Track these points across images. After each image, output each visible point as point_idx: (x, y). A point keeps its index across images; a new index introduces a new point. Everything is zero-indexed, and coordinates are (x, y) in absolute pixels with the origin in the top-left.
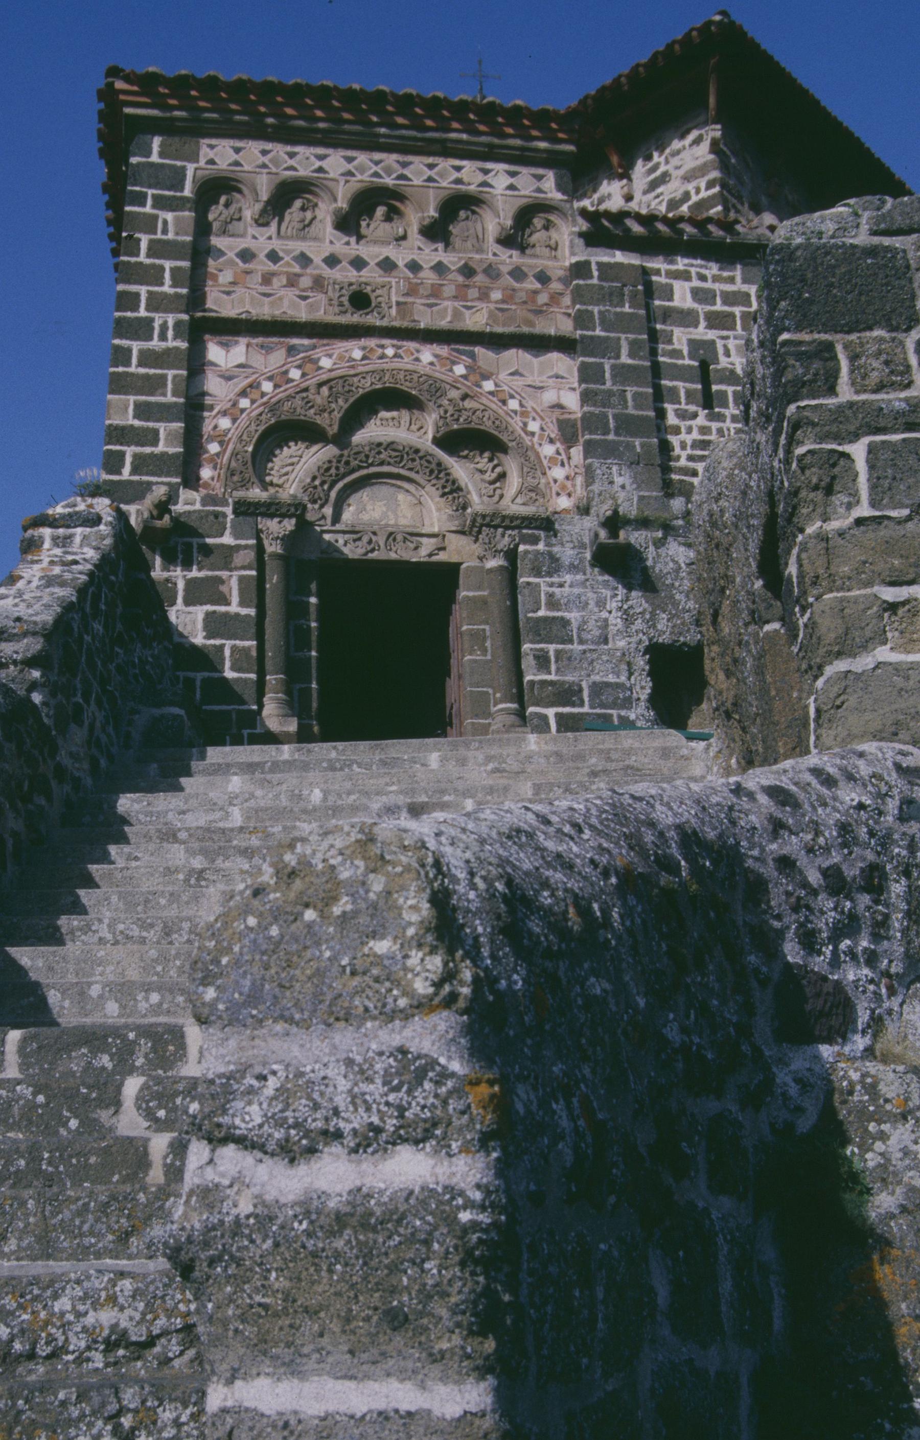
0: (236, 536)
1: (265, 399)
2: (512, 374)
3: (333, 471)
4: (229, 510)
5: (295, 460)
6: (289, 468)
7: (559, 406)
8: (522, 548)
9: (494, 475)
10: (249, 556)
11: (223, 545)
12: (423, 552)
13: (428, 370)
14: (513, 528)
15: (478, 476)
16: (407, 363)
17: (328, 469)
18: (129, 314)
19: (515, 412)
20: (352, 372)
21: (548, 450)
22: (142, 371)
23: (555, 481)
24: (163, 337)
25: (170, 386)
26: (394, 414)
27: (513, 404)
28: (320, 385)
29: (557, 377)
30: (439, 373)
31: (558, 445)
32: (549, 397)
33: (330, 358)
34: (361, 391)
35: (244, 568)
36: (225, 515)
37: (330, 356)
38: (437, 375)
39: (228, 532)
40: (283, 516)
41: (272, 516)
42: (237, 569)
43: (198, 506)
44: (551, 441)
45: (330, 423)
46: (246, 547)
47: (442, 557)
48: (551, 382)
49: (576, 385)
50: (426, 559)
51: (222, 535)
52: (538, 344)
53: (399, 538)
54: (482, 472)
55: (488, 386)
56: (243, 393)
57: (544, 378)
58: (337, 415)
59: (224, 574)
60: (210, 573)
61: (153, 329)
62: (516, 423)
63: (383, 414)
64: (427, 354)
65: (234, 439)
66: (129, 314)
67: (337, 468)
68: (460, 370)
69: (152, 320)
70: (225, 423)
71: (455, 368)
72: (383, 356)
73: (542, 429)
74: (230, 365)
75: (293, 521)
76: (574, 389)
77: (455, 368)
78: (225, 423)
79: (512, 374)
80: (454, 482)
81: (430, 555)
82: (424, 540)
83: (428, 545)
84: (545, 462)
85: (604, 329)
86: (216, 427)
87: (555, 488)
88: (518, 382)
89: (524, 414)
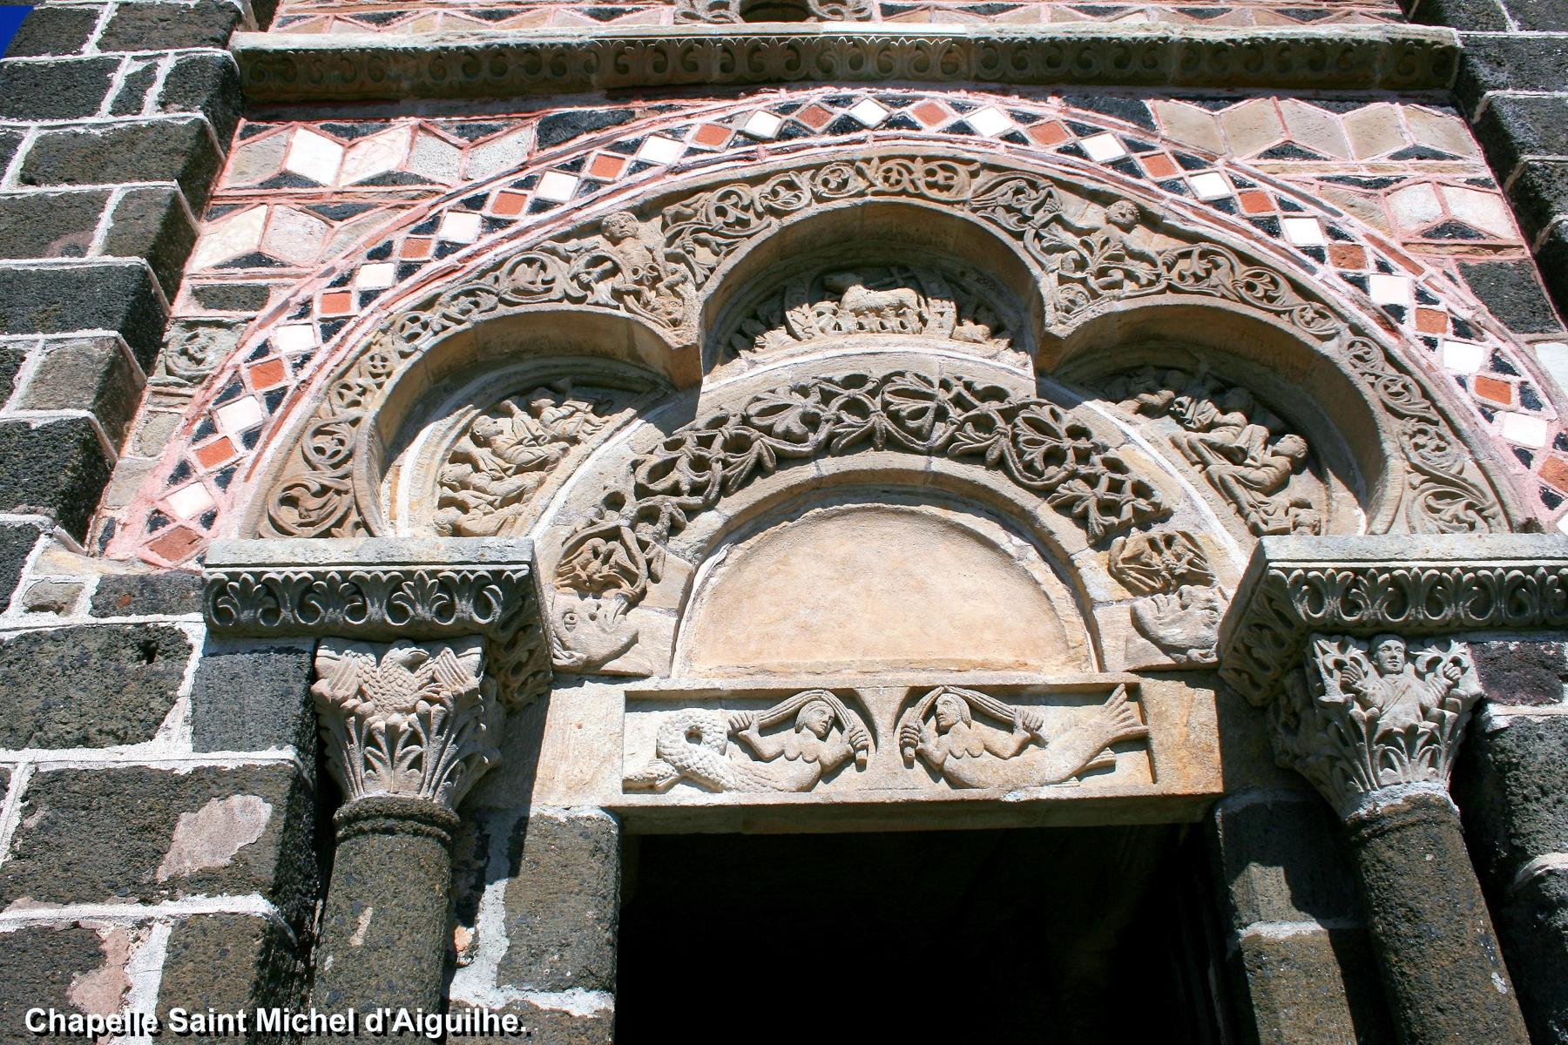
0: (203, 739)
1: (450, 260)
2: (1271, 154)
3: (683, 475)
4: (193, 626)
5: (552, 450)
6: (529, 479)
7: (1452, 230)
8: (1499, 715)
9: (1282, 463)
10: (251, 820)
11: (139, 775)
12: (1053, 763)
13: (1003, 154)
14: (1442, 636)
15: (1220, 466)
16: (931, 138)
17: (668, 466)
18: (46, 58)
19: (1317, 254)
20: (750, 171)
21: (1462, 359)
22: (31, 190)
23: (1525, 456)
24: (130, 101)
25: (105, 221)
26: (907, 295)
27: (1302, 231)
28: (644, 212)
29: (1421, 154)
30: (1041, 156)
31: (1492, 341)
32: (1415, 206)
33: (669, 143)
34: (776, 224)
35: (207, 882)
36: (177, 643)
37: (675, 134)
38: (1030, 164)
39: (177, 719)
40: (429, 639)
41: (376, 641)
42: (175, 888)
43: (81, 615)
44: (1464, 330)
45: (679, 318)
46: (242, 781)
47: (1129, 777)
48: (1408, 167)
49: (1486, 173)
50: (1069, 791)
51: (149, 730)
52: (1335, 75)
53: (953, 708)
54: (1236, 455)
55: (1211, 185)
56: (380, 254)
57: (1382, 159)
58: (694, 301)
59: (109, 916)
60: (45, 914)
61: (108, 85)
62: (1326, 279)
63: (857, 294)
64: (991, 116)
65: (320, 381)
66: (46, 58)
67: (699, 464)
68: (1105, 147)
69: (114, 65)
70: (293, 338)
71: (1087, 144)
72: (847, 125)
73: (1421, 296)
74: (345, 182)
75: (474, 655)
76: (1484, 183)
77: (1087, 144)
78: (293, 338)
79: (1271, 154)
80: (1141, 490)
81: (1081, 774)
82: (1050, 718)
83: (1070, 736)
84: (1467, 399)
85: (1527, 24)
86: (263, 350)
87: (1532, 480)
88: (1298, 173)
89: (1349, 254)
